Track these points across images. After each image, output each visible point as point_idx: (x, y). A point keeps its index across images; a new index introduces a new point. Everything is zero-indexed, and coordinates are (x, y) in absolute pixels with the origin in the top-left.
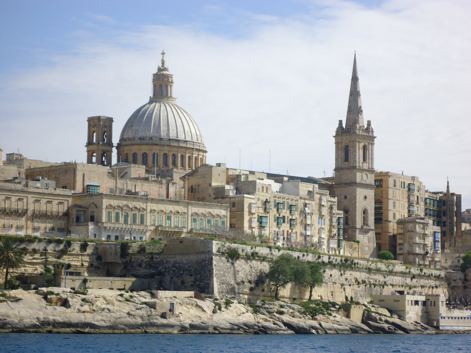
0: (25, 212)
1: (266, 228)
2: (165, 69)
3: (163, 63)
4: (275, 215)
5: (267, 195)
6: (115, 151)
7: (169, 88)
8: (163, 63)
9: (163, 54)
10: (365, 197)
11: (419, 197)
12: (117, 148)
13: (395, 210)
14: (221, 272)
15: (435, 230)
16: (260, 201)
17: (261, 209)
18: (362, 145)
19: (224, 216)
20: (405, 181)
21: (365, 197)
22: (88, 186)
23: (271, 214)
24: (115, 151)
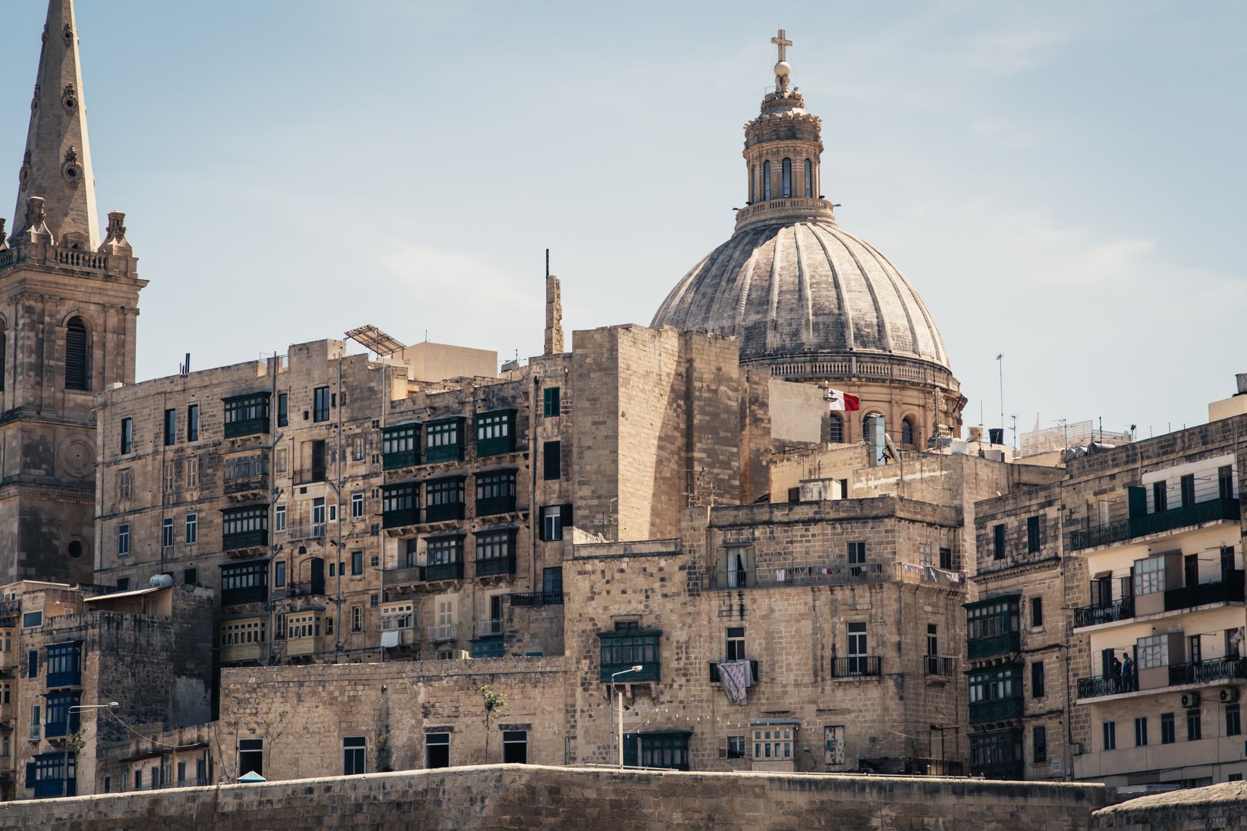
2: (795, 100)
3: (782, 79)
7: (799, 167)
8: (782, 79)
9: (781, 42)
11: (333, 440)
13: (129, 562)
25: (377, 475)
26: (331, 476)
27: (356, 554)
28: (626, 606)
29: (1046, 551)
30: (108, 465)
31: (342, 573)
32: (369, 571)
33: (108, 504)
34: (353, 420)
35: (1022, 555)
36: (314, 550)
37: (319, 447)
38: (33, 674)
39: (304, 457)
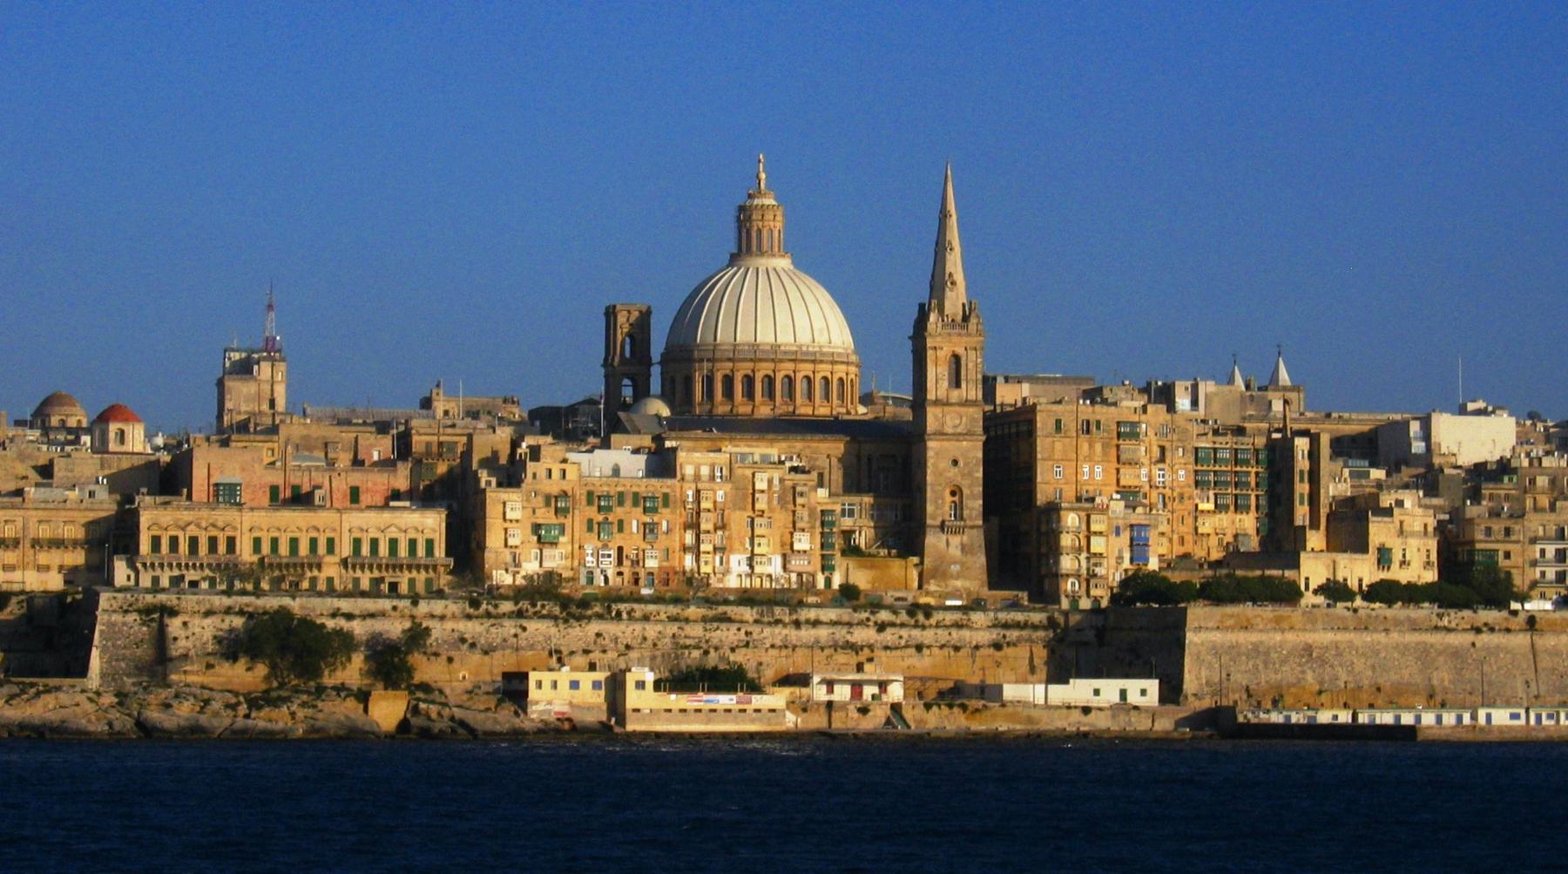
0: (16, 543)
1: (559, 546)
4: (590, 521)
5: (564, 482)
6: (656, 371)
10: (955, 462)
11: (1167, 445)
12: (660, 363)
14: (119, 642)
15: (1134, 522)
16: (540, 499)
17: (543, 510)
18: (945, 353)
19: (434, 531)
20: (1098, 417)
21: (955, 462)
22: (217, 485)
23: (577, 518)
24: (656, 371)
25: (1189, 464)
26: (1168, 461)
27: (1182, 497)
28: (1383, 539)
29: (1513, 538)
30: (1046, 436)
31: (1174, 499)
32: (1186, 501)
33: (1046, 456)
34: (1179, 440)
35: (1501, 536)
36: (1161, 490)
37: (1163, 449)
38: (1118, 534)
39: (1156, 452)
